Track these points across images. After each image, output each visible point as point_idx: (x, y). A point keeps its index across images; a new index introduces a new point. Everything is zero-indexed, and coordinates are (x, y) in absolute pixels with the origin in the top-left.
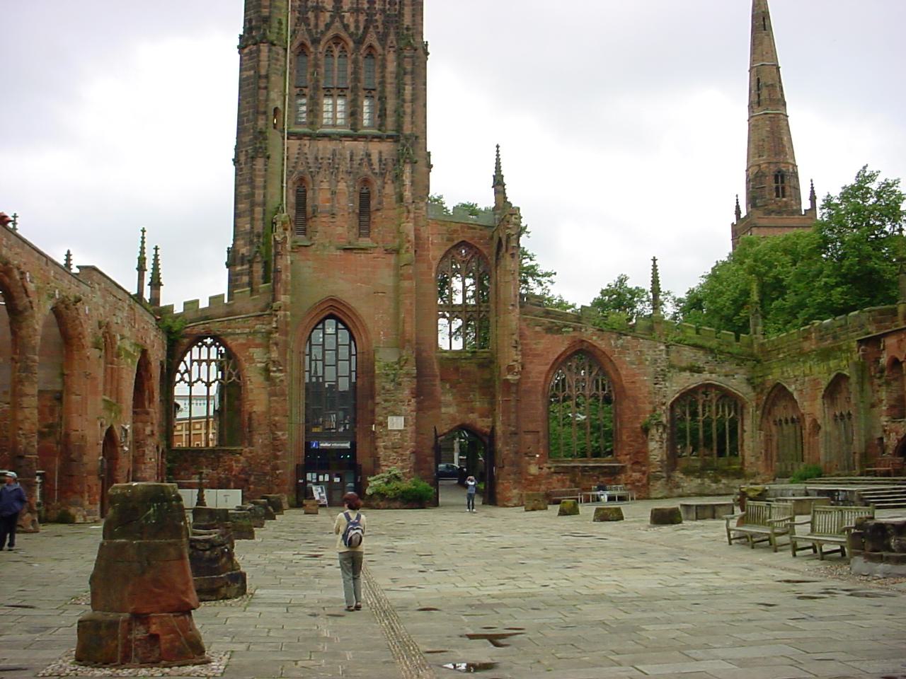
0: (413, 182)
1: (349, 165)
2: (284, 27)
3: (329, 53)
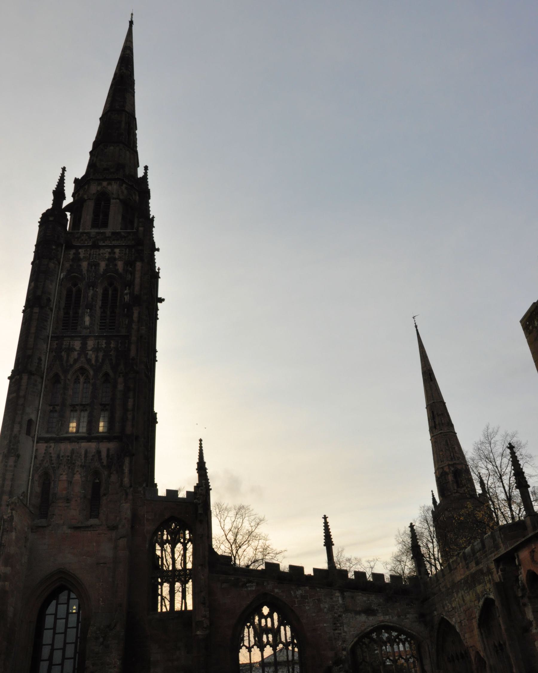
0: (130, 471)
1: (83, 461)
2: (43, 362)
3: (77, 381)
